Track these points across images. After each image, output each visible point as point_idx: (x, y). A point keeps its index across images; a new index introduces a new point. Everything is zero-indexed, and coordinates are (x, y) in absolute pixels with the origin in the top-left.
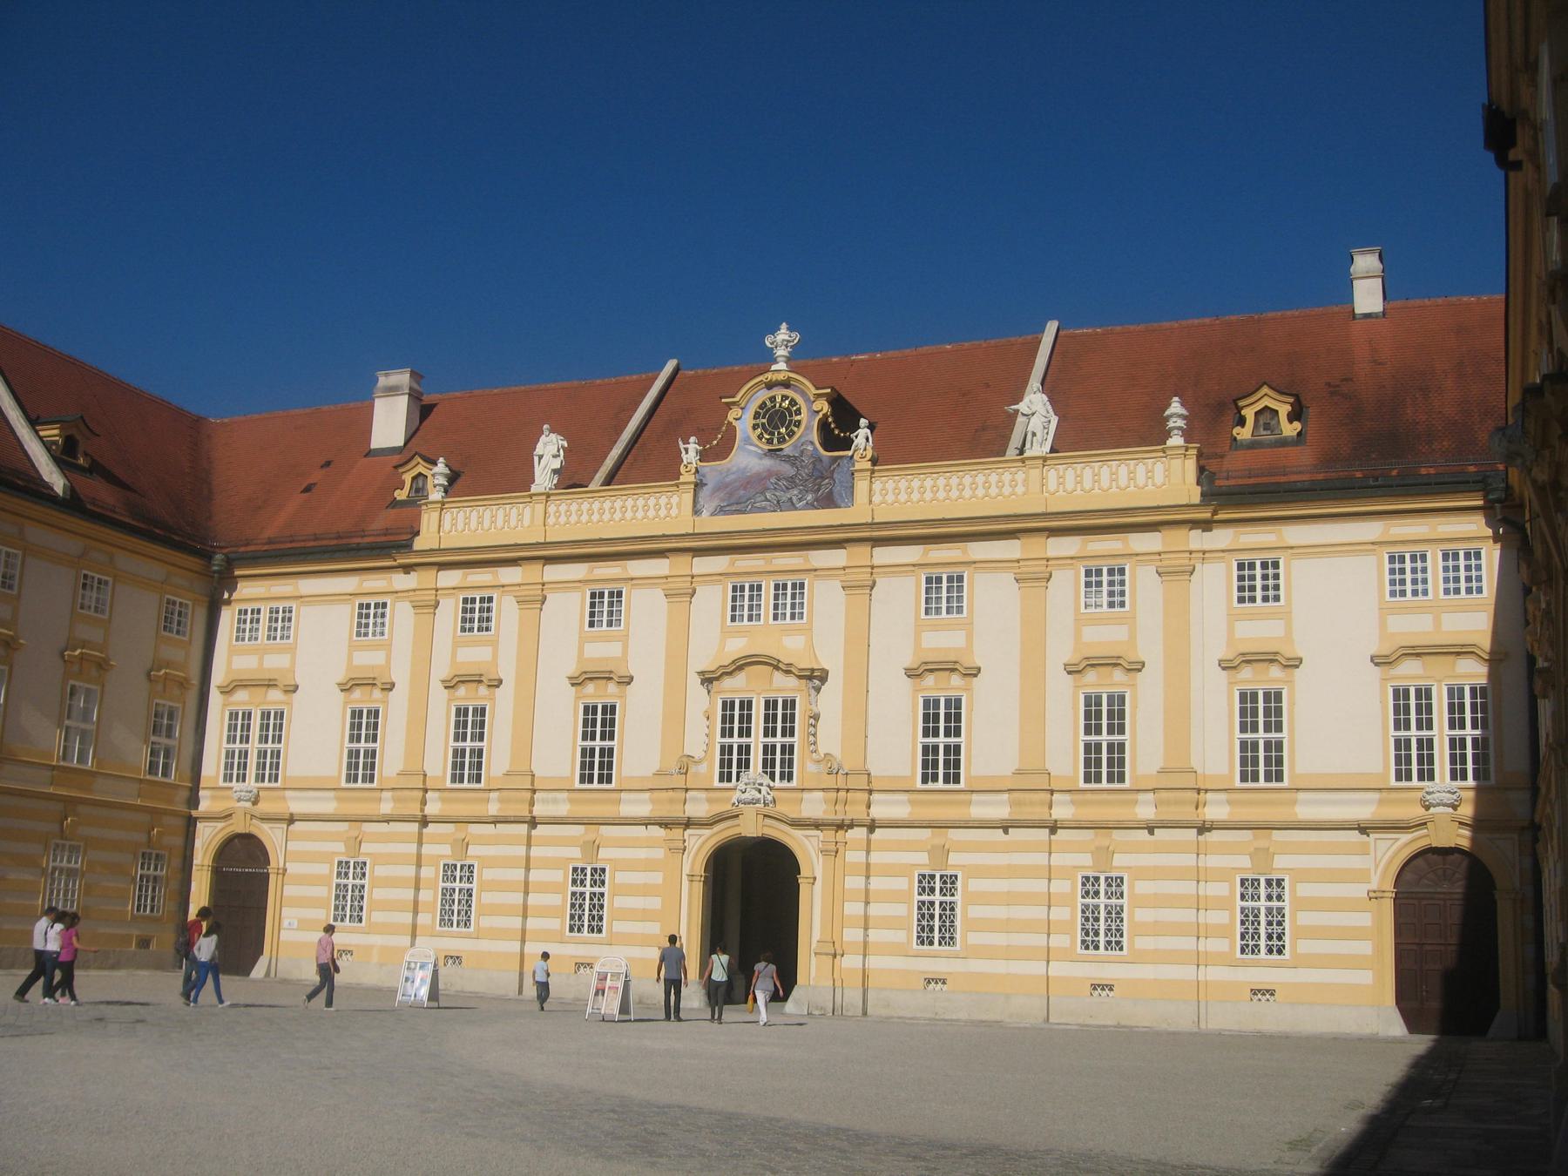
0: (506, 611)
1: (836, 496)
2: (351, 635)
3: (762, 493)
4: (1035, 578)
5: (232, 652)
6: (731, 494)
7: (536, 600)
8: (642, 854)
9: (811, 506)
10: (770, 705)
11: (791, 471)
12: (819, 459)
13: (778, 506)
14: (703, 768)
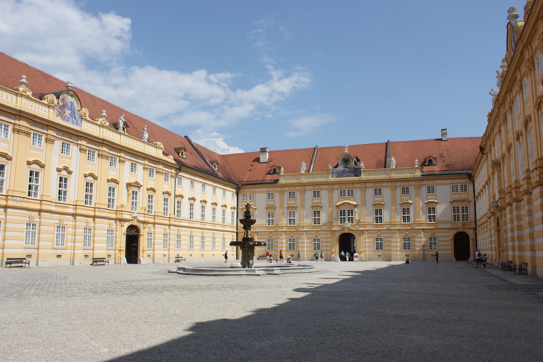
0: (298, 194)
1: (358, 175)
2: (267, 199)
4: (394, 189)
6: (338, 174)
7: (303, 192)
8: (326, 236)
11: (349, 170)
12: (354, 168)
13: (347, 176)
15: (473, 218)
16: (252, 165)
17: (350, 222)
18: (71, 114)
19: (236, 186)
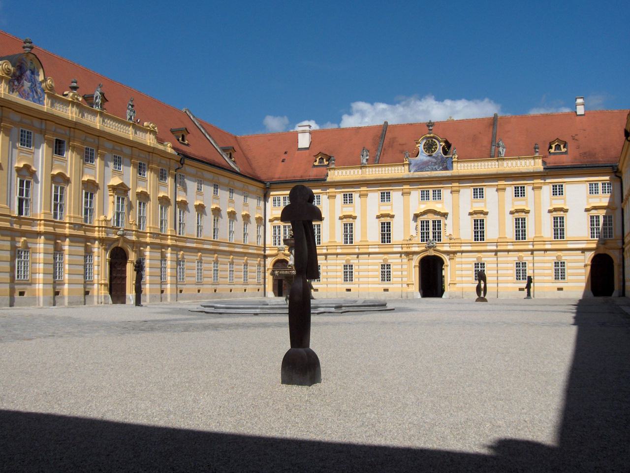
3: (428, 166)
5: (272, 210)
6: (419, 167)
10: (434, 222)
12: (443, 158)
13: (432, 170)
14: (416, 238)
15: (619, 233)
16: (286, 153)
17: (436, 240)
18: (31, 88)
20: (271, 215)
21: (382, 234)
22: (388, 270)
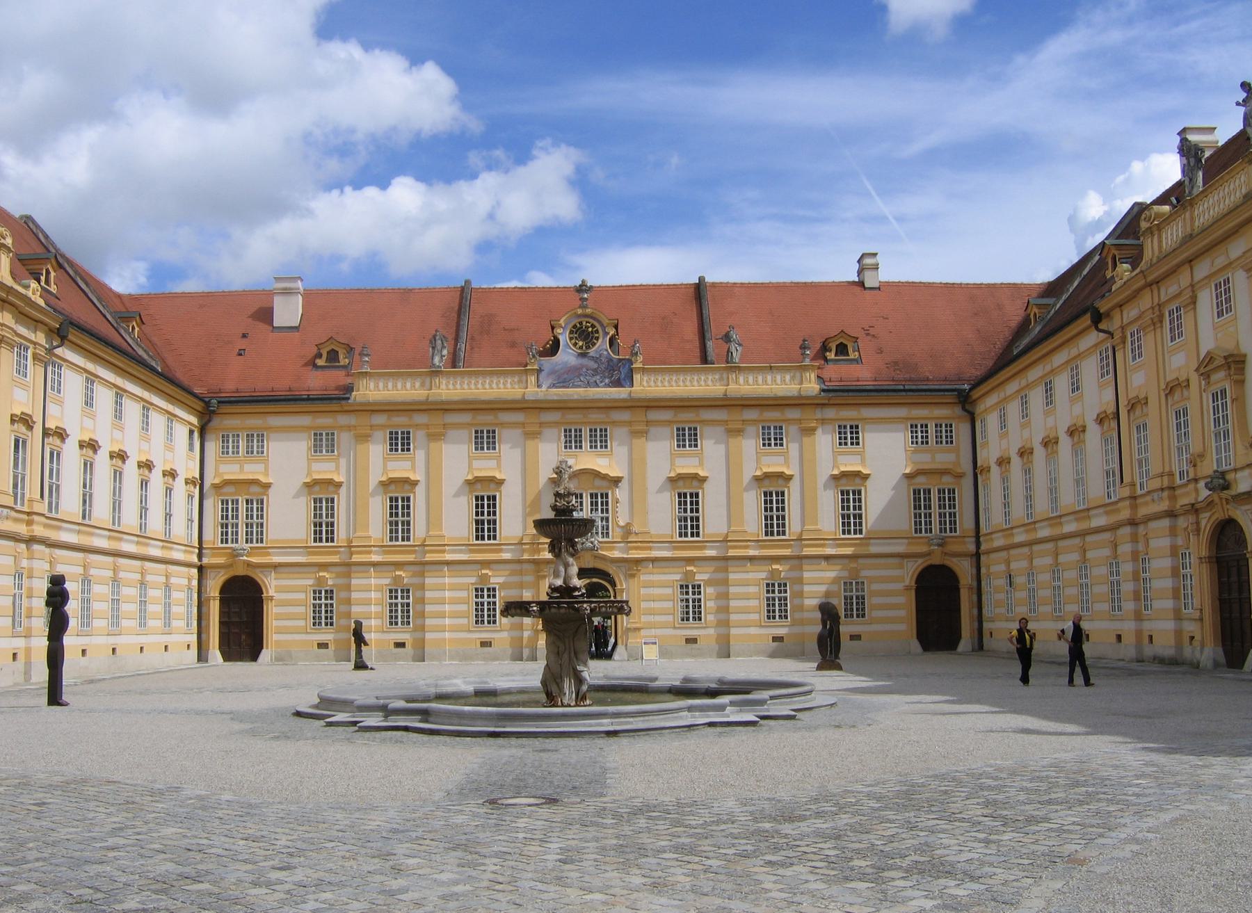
1: (623, 382)
3: (578, 377)
6: (559, 377)
9: (608, 386)
11: (596, 366)
12: (610, 360)
13: (588, 385)
19: (199, 406)
20: (217, 474)
21: (477, 522)
22: (491, 600)
